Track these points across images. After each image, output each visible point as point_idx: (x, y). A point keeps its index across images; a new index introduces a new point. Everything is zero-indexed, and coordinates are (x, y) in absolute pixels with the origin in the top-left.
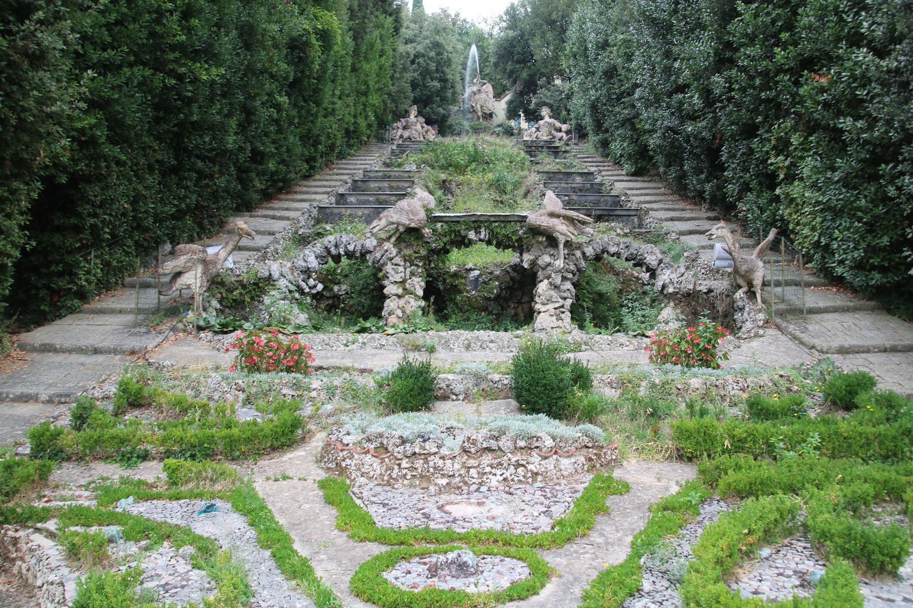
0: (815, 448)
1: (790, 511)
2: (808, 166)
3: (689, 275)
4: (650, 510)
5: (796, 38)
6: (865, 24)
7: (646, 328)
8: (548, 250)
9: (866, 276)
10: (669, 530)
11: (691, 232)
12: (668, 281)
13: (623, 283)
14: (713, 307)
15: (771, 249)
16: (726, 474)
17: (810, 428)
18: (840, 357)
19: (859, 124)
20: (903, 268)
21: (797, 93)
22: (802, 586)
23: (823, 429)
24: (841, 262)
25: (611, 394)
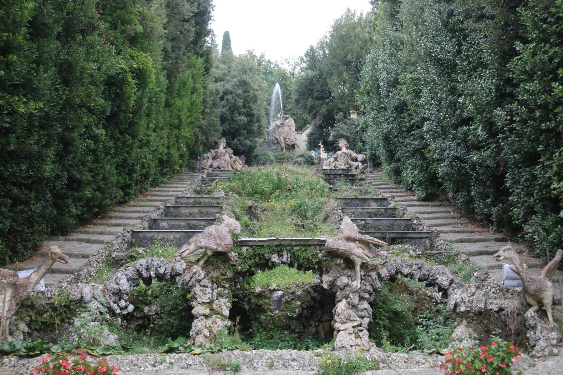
3: (480, 294)
7: (440, 347)
8: (346, 271)
11: (480, 253)
12: (459, 300)
13: (417, 302)
14: (505, 324)
15: (559, 269)
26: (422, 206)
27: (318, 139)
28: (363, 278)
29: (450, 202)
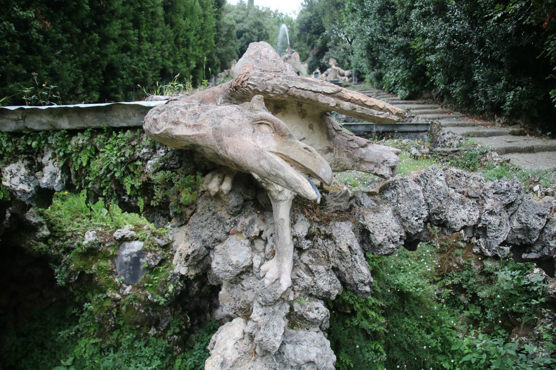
8: (244, 220)
26: (406, 103)
27: (316, 65)
28: (306, 244)
29: (434, 100)
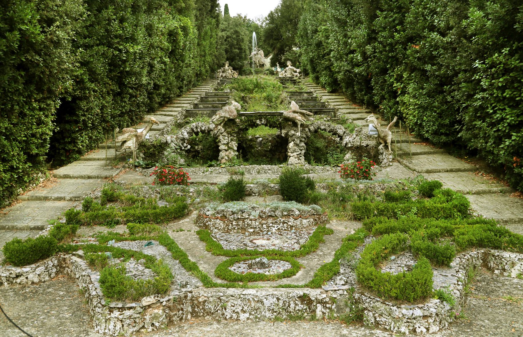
0: (415, 214)
1: (403, 240)
2: (410, 88)
3: (358, 138)
4: (342, 241)
5: (405, 27)
6: (436, 21)
7: (338, 163)
9: (439, 138)
10: (351, 249)
11: (358, 119)
12: (348, 141)
13: (328, 143)
14: (369, 153)
15: (395, 126)
16: (375, 225)
17: (413, 205)
18: (427, 174)
19: (434, 68)
20: (455, 133)
21: (406, 54)
22: (408, 270)
23: (418, 205)
24: (427, 132)
25: (324, 192)
